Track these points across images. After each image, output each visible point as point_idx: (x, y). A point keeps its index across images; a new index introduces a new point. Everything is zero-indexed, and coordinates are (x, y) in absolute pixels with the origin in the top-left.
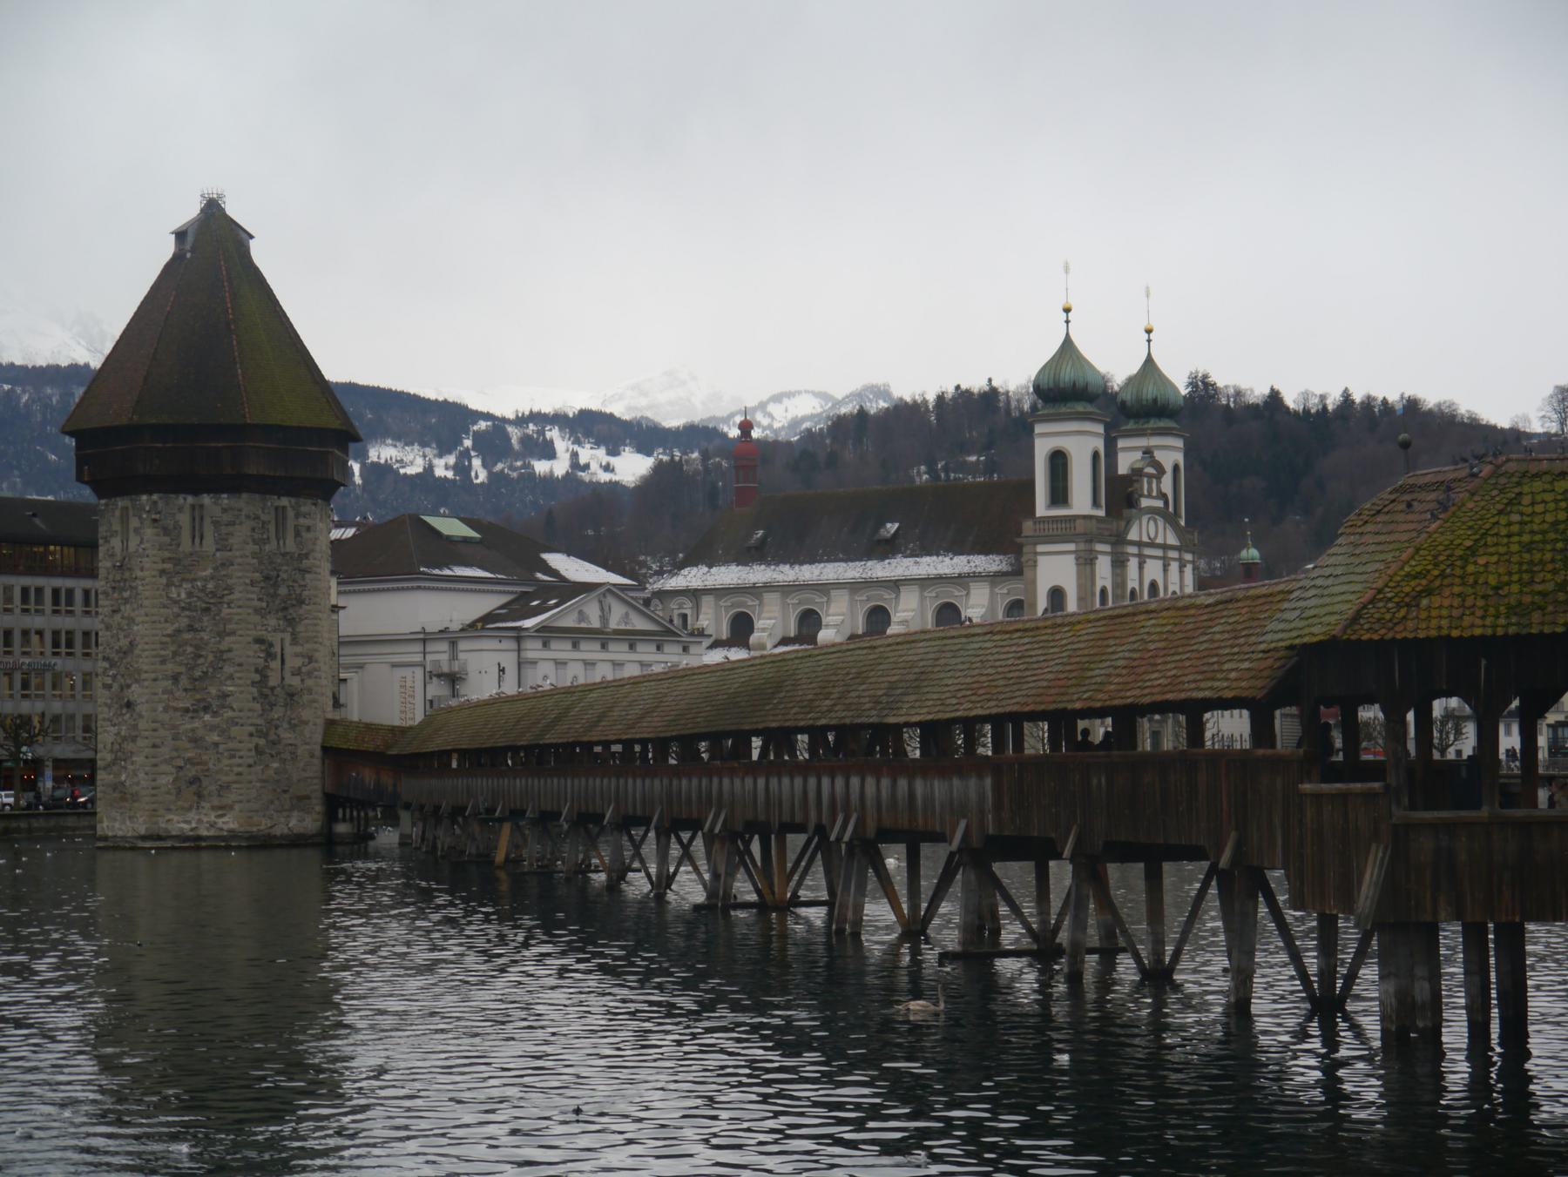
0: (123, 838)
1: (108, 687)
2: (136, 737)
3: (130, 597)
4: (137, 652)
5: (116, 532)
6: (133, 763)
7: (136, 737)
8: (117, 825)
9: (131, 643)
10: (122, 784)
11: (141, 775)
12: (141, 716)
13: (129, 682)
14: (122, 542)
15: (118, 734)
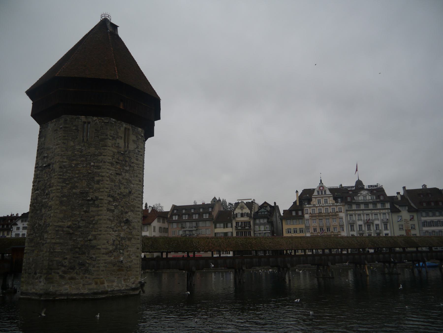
0: (120, 291)
1: (113, 211)
2: (132, 238)
3: (129, 170)
4: (132, 197)
5: (121, 137)
6: (127, 252)
7: (132, 238)
8: (115, 284)
9: (130, 192)
10: (122, 262)
11: (133, 257)
12: (134, 228)
13: (126, 210)
14: (125, 143)
15: (118, 236)
